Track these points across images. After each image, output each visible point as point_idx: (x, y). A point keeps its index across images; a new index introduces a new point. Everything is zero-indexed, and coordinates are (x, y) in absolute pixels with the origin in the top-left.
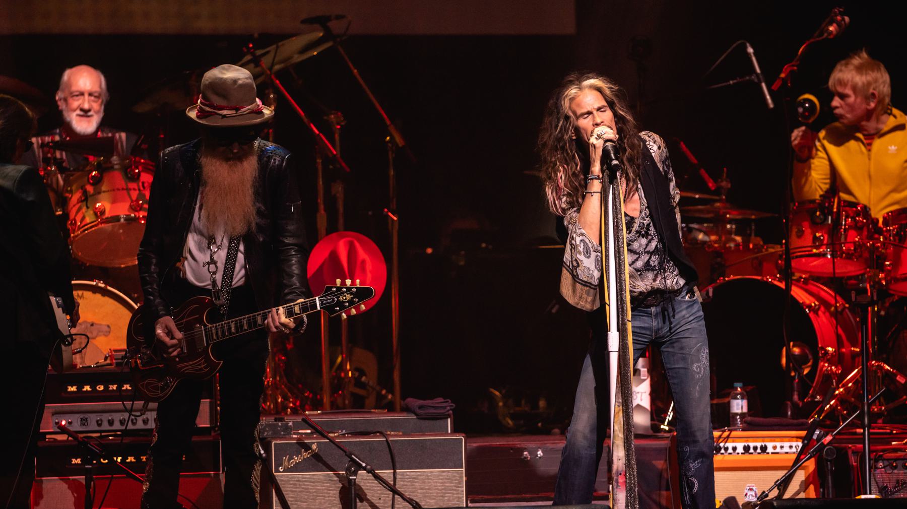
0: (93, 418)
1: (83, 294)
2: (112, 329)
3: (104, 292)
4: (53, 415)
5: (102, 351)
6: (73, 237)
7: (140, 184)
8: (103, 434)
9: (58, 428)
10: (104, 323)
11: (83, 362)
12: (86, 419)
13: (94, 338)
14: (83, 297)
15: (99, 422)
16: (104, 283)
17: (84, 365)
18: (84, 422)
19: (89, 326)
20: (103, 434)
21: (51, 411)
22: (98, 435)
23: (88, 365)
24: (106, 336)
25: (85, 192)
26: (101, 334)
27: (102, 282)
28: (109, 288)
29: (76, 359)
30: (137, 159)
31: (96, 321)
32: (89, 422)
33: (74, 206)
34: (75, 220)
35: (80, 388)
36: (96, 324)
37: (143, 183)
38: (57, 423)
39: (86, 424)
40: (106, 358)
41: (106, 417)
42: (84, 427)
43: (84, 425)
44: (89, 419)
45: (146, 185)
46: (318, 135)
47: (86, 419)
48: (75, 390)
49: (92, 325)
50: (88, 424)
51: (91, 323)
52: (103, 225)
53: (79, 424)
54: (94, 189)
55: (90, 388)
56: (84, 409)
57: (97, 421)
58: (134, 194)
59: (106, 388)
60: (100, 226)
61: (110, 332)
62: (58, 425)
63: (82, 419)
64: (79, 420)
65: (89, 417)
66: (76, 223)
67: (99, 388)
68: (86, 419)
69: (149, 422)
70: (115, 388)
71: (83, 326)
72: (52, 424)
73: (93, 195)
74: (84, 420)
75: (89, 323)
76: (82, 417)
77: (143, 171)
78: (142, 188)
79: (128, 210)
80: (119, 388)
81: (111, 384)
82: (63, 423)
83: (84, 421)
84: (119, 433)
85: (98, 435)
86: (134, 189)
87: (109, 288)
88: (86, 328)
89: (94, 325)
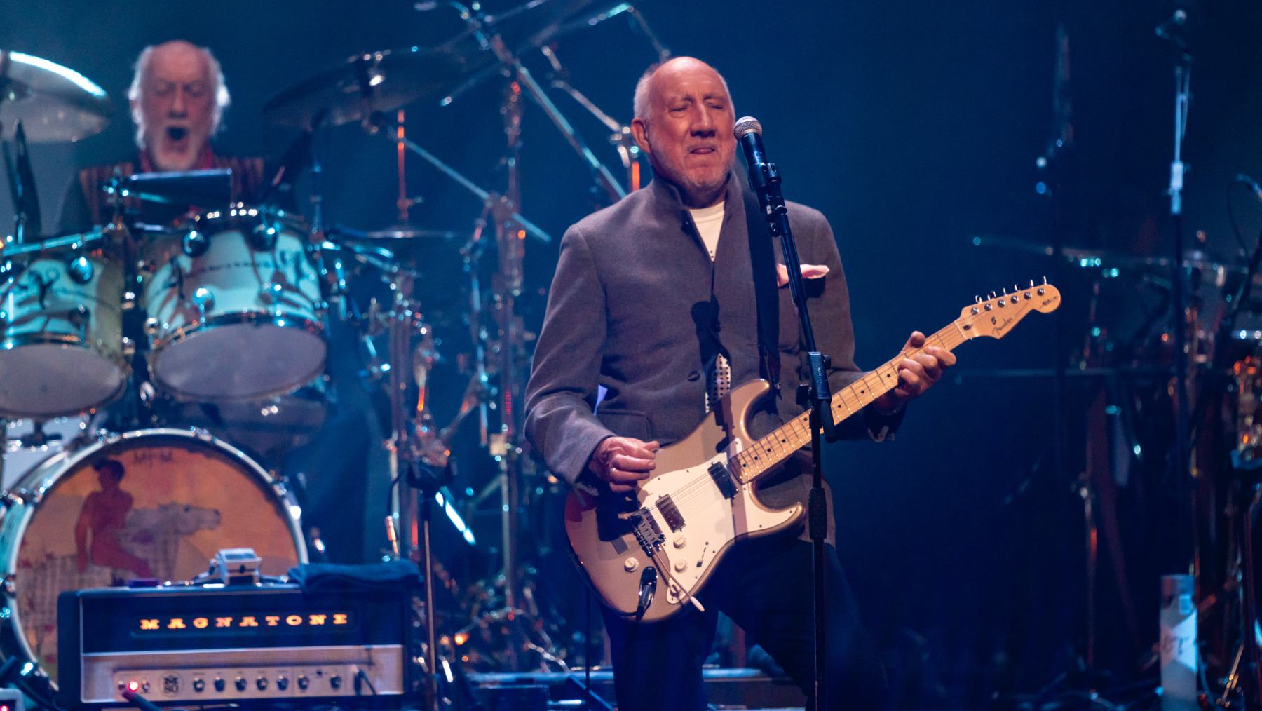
3: (210, 449)
7: (278, 256)
9: (125, 695)
12: (175, 680)
13: (191, 533)
15: (199, 686)
16: (211, 433)
18: (171, 684)
20: (206, 707)
21: (111, 664)
24: (211, 529)
25: (178, 271)
30: (272, 210)
32: (180, 685)
33: (158, 293)
35: (164, 624)
37: (283, 254)
38: (121, 687)
39: (175, 688)
41: (212, 676)
42: (171, 694)
43: (170, 690)
44: (179, 681)
45: (288, 257)
46: (598, 170)
49: (187, 509)
50: (177, 688)
54: (193, 265)
55: (183, 623)
58: (267, 273)
59: (212, 623)
62: (123, 691)
63: (167, 680)
64: (162, 681)
65: (179, 675)
67: (199, 623)
68: (175, 680)
69: (289, 686)
72: (113, 689)
74: (171, 682)
76: (166, 676)
78: (279, 263)
79: (256, 302)
80: (235, 624)
82: (134, 686)
83: (171, 684)
84: (234, 705)
86: (266, 265)
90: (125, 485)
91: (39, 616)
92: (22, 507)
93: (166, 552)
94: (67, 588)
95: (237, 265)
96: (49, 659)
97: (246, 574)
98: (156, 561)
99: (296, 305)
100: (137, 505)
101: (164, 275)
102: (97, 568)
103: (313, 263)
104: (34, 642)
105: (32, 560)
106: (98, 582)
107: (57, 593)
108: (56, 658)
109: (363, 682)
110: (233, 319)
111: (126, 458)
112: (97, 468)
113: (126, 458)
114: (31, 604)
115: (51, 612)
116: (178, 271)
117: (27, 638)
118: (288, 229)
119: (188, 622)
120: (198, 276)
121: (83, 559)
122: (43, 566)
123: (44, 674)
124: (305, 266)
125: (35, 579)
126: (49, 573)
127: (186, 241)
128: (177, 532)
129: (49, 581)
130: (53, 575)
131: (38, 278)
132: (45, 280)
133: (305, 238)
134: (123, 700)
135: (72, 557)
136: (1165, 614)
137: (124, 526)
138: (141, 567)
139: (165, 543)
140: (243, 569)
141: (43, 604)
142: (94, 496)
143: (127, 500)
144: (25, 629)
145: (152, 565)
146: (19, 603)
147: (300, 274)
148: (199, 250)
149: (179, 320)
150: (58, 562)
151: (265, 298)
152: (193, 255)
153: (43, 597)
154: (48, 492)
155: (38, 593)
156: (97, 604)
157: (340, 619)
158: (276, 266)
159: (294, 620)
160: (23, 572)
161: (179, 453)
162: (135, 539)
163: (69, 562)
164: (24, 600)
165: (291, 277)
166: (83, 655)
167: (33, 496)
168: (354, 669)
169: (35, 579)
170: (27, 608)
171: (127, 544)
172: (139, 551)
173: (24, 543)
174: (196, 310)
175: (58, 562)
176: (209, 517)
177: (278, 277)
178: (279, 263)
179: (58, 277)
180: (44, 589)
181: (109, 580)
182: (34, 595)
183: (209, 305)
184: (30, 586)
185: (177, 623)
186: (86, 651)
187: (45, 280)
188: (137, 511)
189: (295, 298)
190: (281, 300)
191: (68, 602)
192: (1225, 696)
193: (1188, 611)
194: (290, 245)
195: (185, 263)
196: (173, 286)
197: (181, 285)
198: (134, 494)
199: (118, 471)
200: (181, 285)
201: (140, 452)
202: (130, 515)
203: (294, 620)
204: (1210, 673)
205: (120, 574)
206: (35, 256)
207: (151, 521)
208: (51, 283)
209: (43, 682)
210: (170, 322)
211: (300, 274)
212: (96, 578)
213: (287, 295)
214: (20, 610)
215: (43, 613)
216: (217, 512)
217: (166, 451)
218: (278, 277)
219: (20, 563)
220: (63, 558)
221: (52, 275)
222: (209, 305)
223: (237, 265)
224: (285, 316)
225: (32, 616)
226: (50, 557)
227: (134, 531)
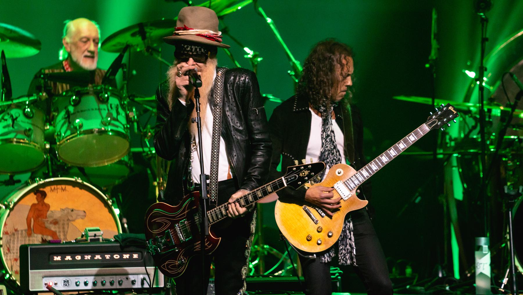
0: (73, 280)
1: (65, 187)
2: (87, 214)
3: (82, 186)
4: (43, 278)
5: (80, 230)
6: (59, 145)
7: (109, 106)
8: (80, 292)
9: (47, 288)
10: (82, 209)
11: (65, 238)
13: (74, 220)
14: (66, 190)
16: (82, 179)
17: (67, 241)
19: (70, 211)
20: (80, 292)
21: (42, 275)
22: (77, 293)
23: (69, 240)
24: (82, 219)
25: (68, 112)
26: (79, 217)
27: (80, 179)
28: (85, 183)
29: (60, 235)
30: (107, 87)
31: (74, 208)
33: (60, 121)
34: (60, 131)
35: (63, 258)
36: (75, 210)
38: (46, 284)
39: (68, 285)
40: (82, 236)
45: (113, 106)
47: (68, 281)
48: (60, 259)
49: (72, 210)
51: (71, 210)
52: (81, 136)
53: (63, 285)
54: (74, 110)
56: (66, 274)
57: (76, 283)
58: (105, 113)
59: (83, 258)
60: (79, 136)
61: (85, 216)
62: (46, 286)
63: (64, 281)
66: (61, 134)
67: (78, 258)
68: (68, 281)
69: (115, 284)
70: (89, 258)
71: (66, 212)
73: (74, 113)
75: (70, 209)
76: (64, 279)
77: (111, 96)
78: (110, 108)
79: (100, 126)
81: (86, 255)
83: (66, 283)
84: (92, 292)
85: (77, 293)
86: (104, 109)
87: (85, 183)
88: (68, 213)
89: (74, 211)
90: (46, 201)
91: (12, 254)
92: (5, 210)
93: (64, 228)
94: (23, 243)
95: (92, 109)
96: (16, 272)
97: (96, 237)
98: (60, 232)
99: (117, 126)
100: (52, 209)
101: (63, 114)
102: (35, 235)
103: (123, 108)
104: (10, 266)
105: (8, 232)
106: (36, 240)
107: (19, 245)
108: (19, 272)
109: (145, 282)
110: (91, 132)
111: (47, 190)
112: (35, 194)
113: (47, 190)
114: (9, 250)
115: (17, 253)
116: (68, 112)
117: (7, 264)
118: (113, 95)
119: (73, 258)
120: (78, 114)
121: (30, 232)
122: (14, 234)
123: (14, 279)
124: (120, 110)
125: (10, 240)
126: (16, 236)
127: (71, 99)
128: (68, 220)
129: (16, 240)
130: (18, 238)
131: (12, 116)
132: (14, 117)
133: (120, 98)
134: (47, 290)
135: (25, 230)
136: (477, 254)
137: (46, 217)
138: (54, 234)
139: (63, 224)
140: (95, 235)
141: (13, 250)
142: (34, 205)
143: (48, 207)
144: (7, 260)
145: (58, 234)
146: (4, 249)
147: (118, 113)
148: (77, 103)
149: (69, 132)
150: (20, 232)
151: (104, 124)
152: (75, 105)
153: (14, 247)
154: (15, 204)
155: (12, 245)
156: (36, 251)
157: (135, 256)
158: (108, 110)
159: (117, 257)
160: (5, 236)
161: (69, 188)
162: (51, 223)
163: (24, 232)
164: (6, 248)
165: (115, 115)
166: (30, 271)
167: (9, 205)
168: (142, 276)
170: (7, 252)
171: (47, 225)
172: (53, 228)
173: (5, 224)
174: (76, 128)
175: (20, 232)
176: (82, 214)
177: (109, 115)
178: (110, 108)
179: (19, 115)
180: (14, 244)
181: (41, 240)
182: (10, 245)
183: (81, 126)
184: (8, 242)
185: (68, 258)
186: (31, 270)
187: (14, 117)
188: (52, 211)
189: (116, 123)
190: (110, 124)
191: (23, 249)
192: (502, 287)
193: (486, 252)
194: (114, 101)
195: (71, 109)
196: (66, 118)
197: (69, 118)
198: (50, 204)
199: (44, 195)
200: (69, 118)
201: (53, 187)
202: (49, 213)
203: (117, 257)
204: (496, 279)
205: (45, 237)
206: (9, 107)
207: (57, 215)
208: (16, 118)
209: (14, 282)
210: (65, 133)
211: (118, 113)
212: (35, 239)
213: (113, 122)
214: (4, 252)
215: (14, 253)
216: (85, 212)
217: (63, 186)
218: (109, 115)
219: (4, 233)
220: (22, 231)
221: (17, 115)
222: (81, 126)
223: (92, 109)
224: (112, 131)
225: (9, 254)
226: (16, 230)
227: (50, 220)
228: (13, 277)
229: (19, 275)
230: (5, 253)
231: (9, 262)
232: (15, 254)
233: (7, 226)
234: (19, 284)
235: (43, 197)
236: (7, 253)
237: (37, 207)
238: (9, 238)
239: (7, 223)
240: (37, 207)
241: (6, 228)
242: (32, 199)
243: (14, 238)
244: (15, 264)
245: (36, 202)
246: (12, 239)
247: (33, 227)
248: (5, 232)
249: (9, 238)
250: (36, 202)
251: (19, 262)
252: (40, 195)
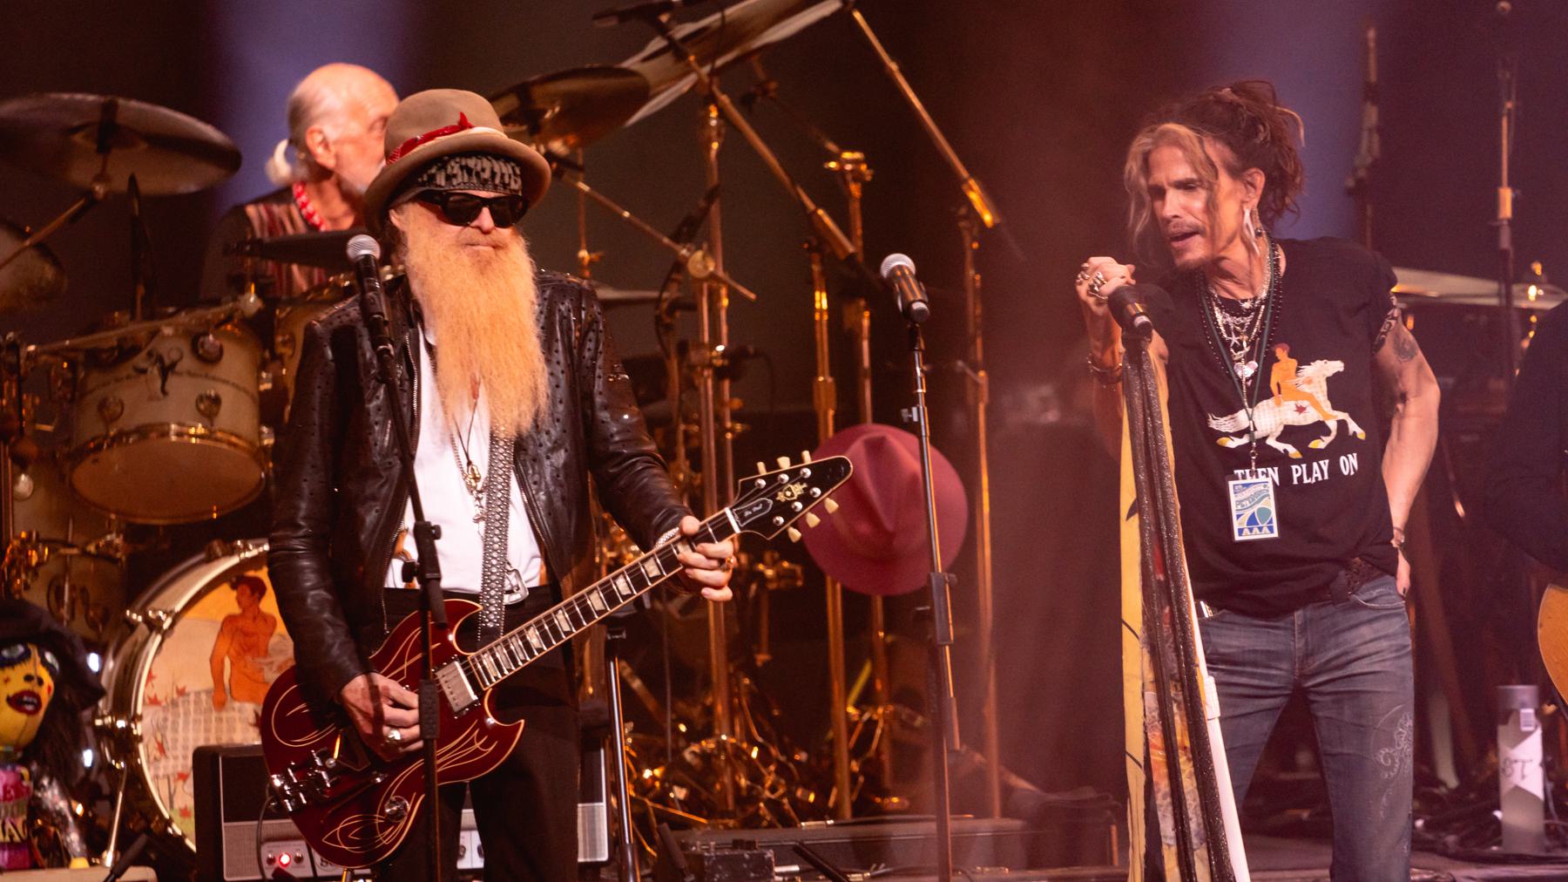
96: (184, 813)
102: (237, 705)
105: (159, 698)
112: (234, 587)
115: (185, 757)
122: (174, 704)
123: (179, 832)
125: (165, 720)
126: (181, 710)
130: (187, 714)
131: (160, 359)
132: (167, 362)
135: (207, 692)
137: (266, 653)
141: (175, 748)
142: (230, 620)
146: (147, 747)
150: (192, 697)
153: (175, 741)
155: (169, 735)
163: (203, 697)
164: (153, 745)
169: (165, 720)
170: (158, 754)
173: (150, 677)
175: (192, 697)
180: (175, 730)
182: (163, 736)
187: (167, 362)
215: (176, 758)
219: (147, 700)
220: (198, 694)
221: (175, 355)
226: (181, 692)
228: (174, 826)
229: (193, 819)
230: (152, 758)
231: (163, 784)
232: (181, 761)
233: (154, 682)
234: (193, 847)
235: (257, 595)
236: (155, 759)
237: (240, 624)
238: (161, 715)
239: (154, 673)
240: (240, 624)
241: (153, 686)
242: (226, 601)
243: (177, 715)
244: (179, 789)
245: (236, 610)
246: (170, 718)
247: (230, 681)
248: (150, 699)
249: (161, 715)
250: (235, 609)
251: (190, 781)
252: (248, 591)
